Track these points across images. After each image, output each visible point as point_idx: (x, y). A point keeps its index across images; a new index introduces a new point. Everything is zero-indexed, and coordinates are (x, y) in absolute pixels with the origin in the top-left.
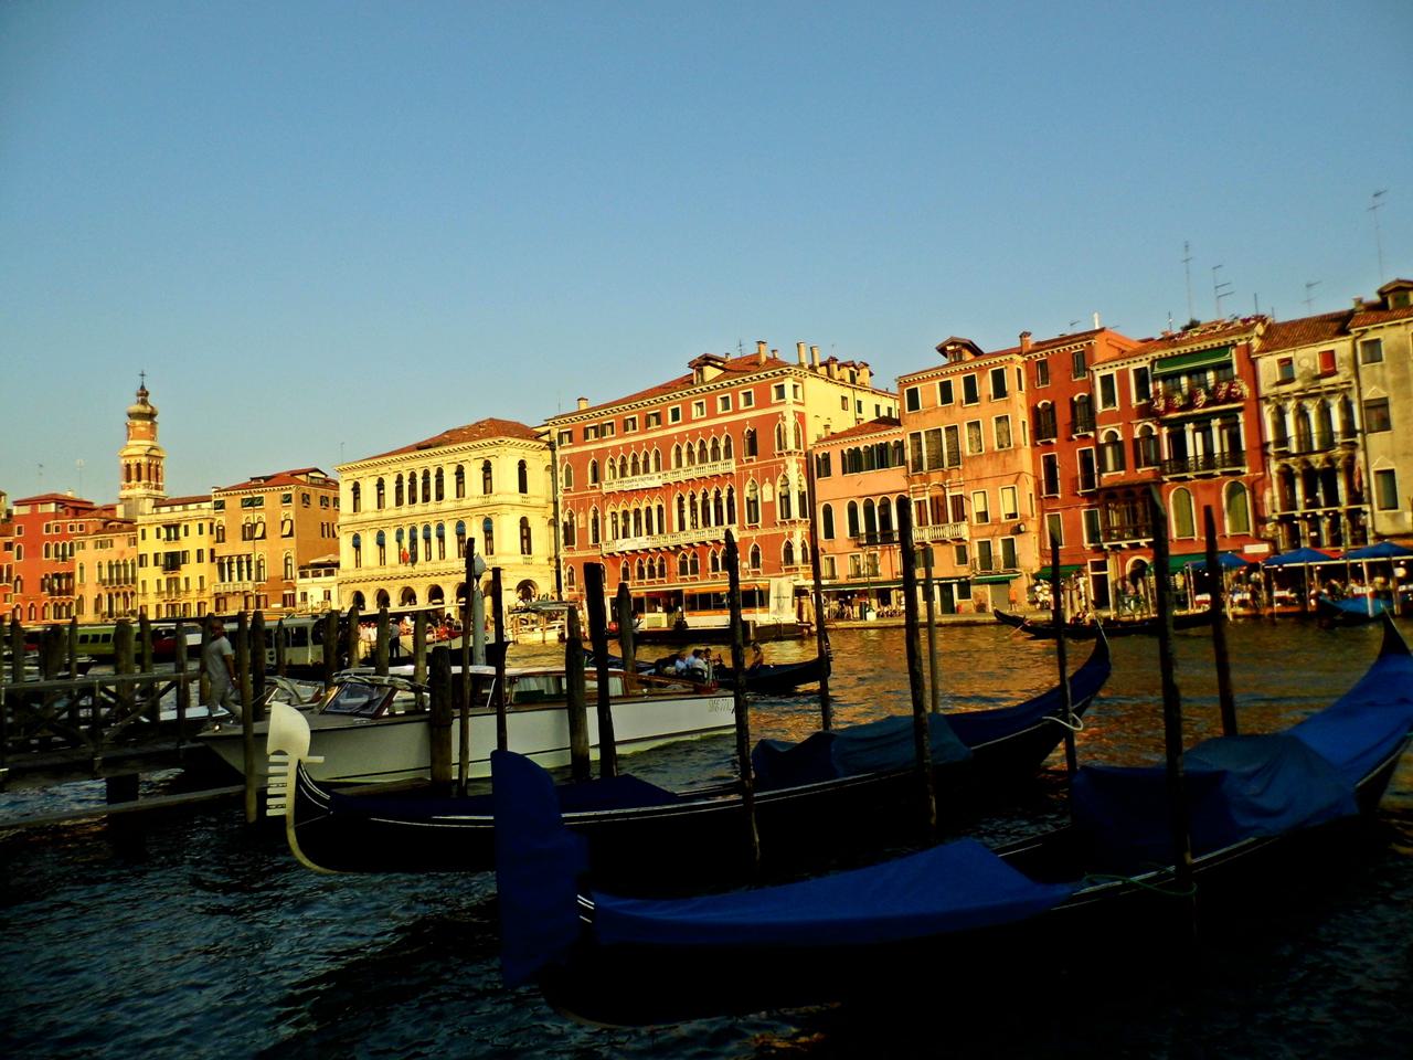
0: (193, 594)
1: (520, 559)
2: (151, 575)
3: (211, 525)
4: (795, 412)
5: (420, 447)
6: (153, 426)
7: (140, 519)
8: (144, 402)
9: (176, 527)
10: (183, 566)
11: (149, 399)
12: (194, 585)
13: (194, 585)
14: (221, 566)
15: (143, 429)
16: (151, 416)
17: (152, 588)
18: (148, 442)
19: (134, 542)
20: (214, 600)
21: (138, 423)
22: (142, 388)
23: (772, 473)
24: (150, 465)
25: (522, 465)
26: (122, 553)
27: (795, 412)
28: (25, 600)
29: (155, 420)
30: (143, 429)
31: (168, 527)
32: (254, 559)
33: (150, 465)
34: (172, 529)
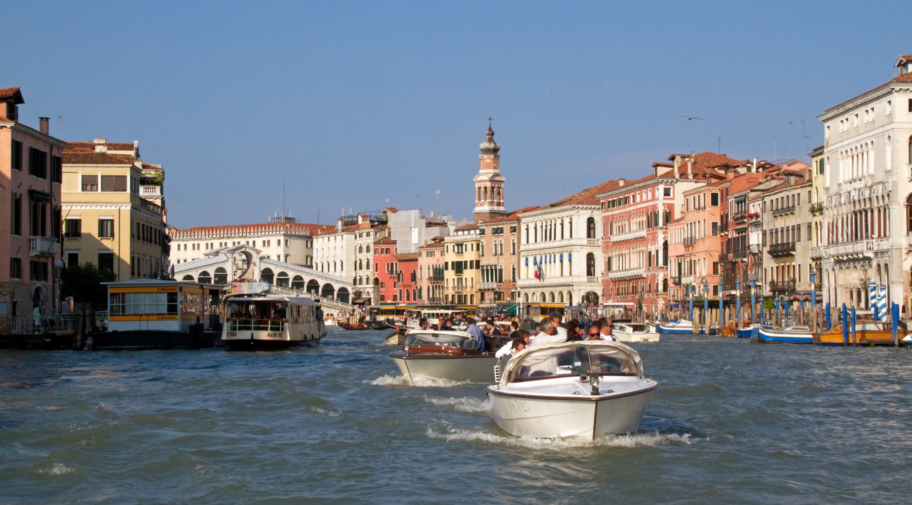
0: (469, 289)
1: (585, 278)
2: (450, 274)
3: (478, 245)
4: (664, 204)
5: (553, 206)
6: (497, 157)
7: (446, 239)
8: (491, 140)
9: (462, 245)
10: (464, 271)
11: (495, 137)
12: (469, 284)
13: (469, 284)
14: (483, 271)
15: (488, 161)
16: (495, 151)
17: (451, 284)
18: (492, 171)
19: (442, 254)
20: (479, 294)
21: (486, 156)
22: (490, 129)
23: (655, 239)
24: (493, 188)
25: (591, 221)
26: (438, 260)
27: (664, 204)
28: (404, 286)
29: (499, 153)
30: (488, 161)
31: (458, 245)
32: (498, 268)
33: (493, 188)
34: (460, 245)
